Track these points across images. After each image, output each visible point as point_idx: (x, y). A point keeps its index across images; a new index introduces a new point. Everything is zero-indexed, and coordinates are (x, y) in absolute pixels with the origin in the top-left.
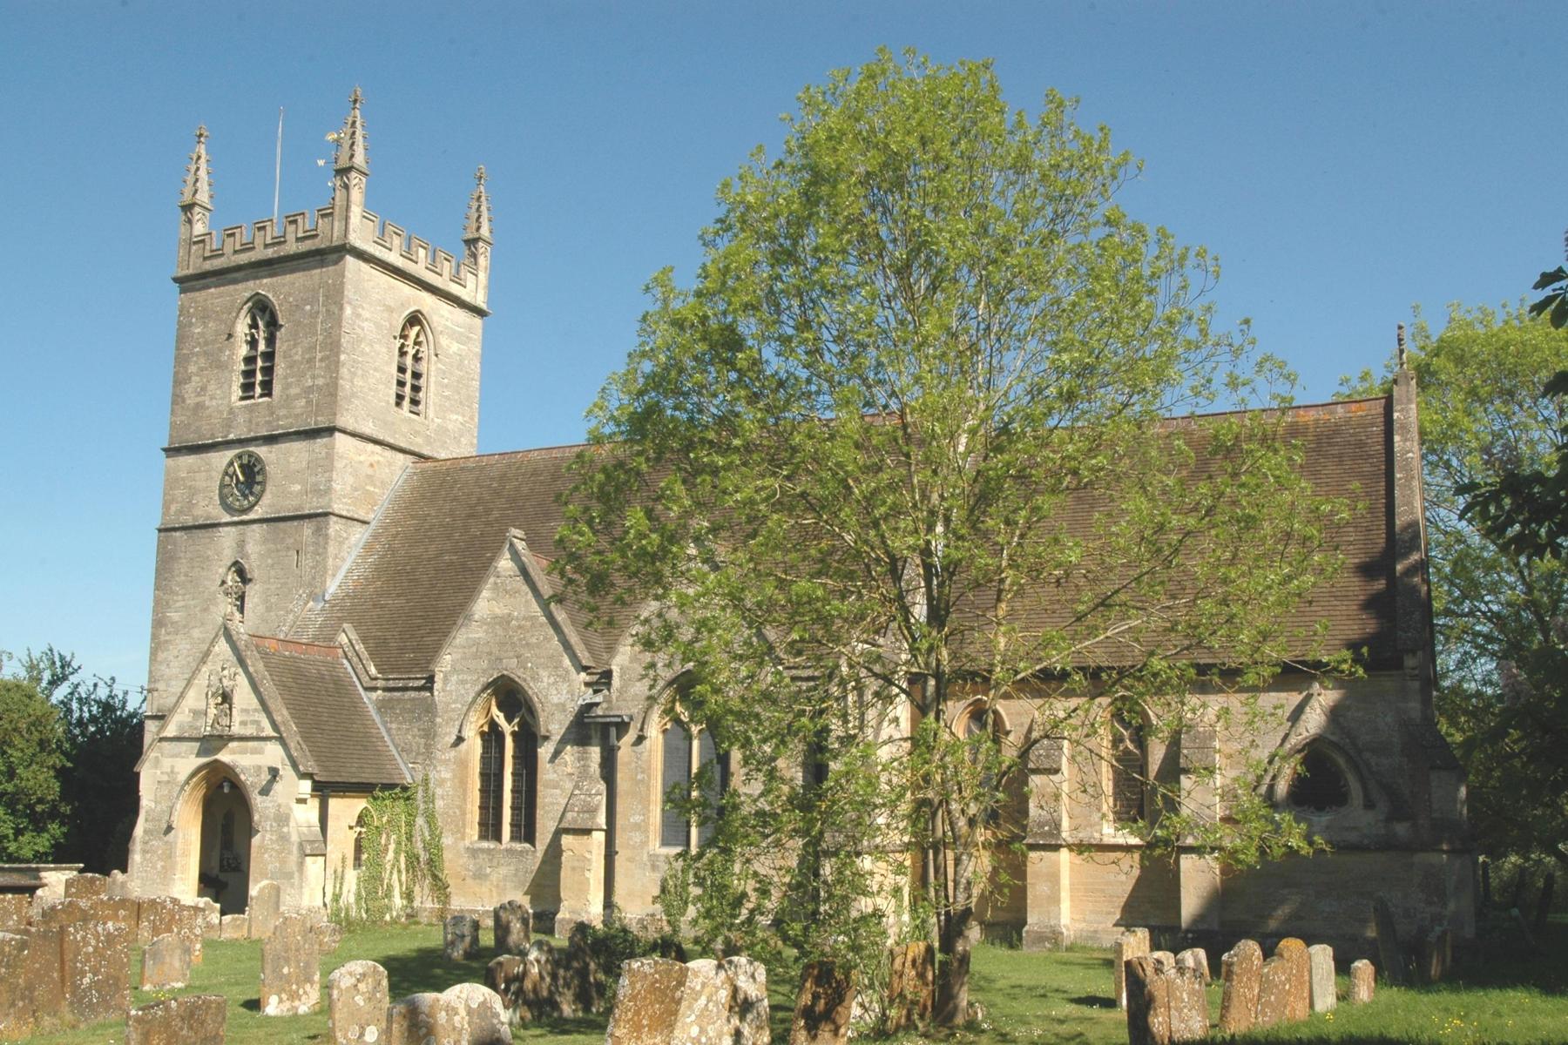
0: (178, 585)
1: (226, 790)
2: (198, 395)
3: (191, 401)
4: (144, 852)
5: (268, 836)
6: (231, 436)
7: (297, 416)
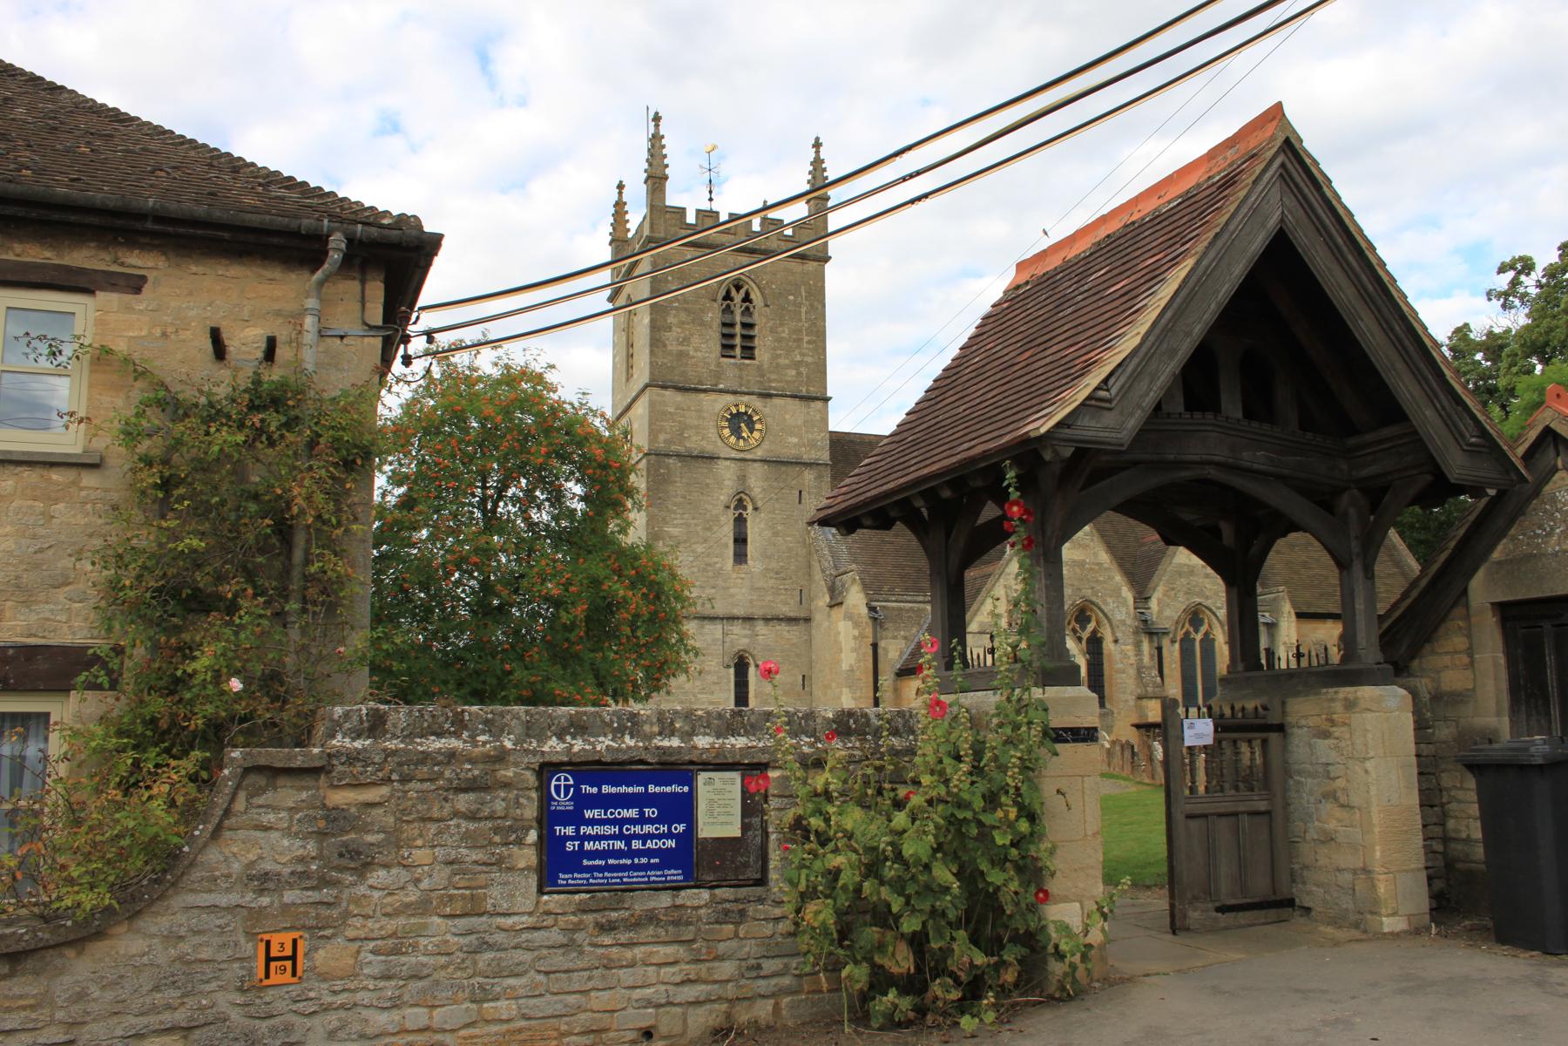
0: (675, 504)
2: (681, 344)
3: (673, 347)
6: (721, 386)
7: (788, 382)
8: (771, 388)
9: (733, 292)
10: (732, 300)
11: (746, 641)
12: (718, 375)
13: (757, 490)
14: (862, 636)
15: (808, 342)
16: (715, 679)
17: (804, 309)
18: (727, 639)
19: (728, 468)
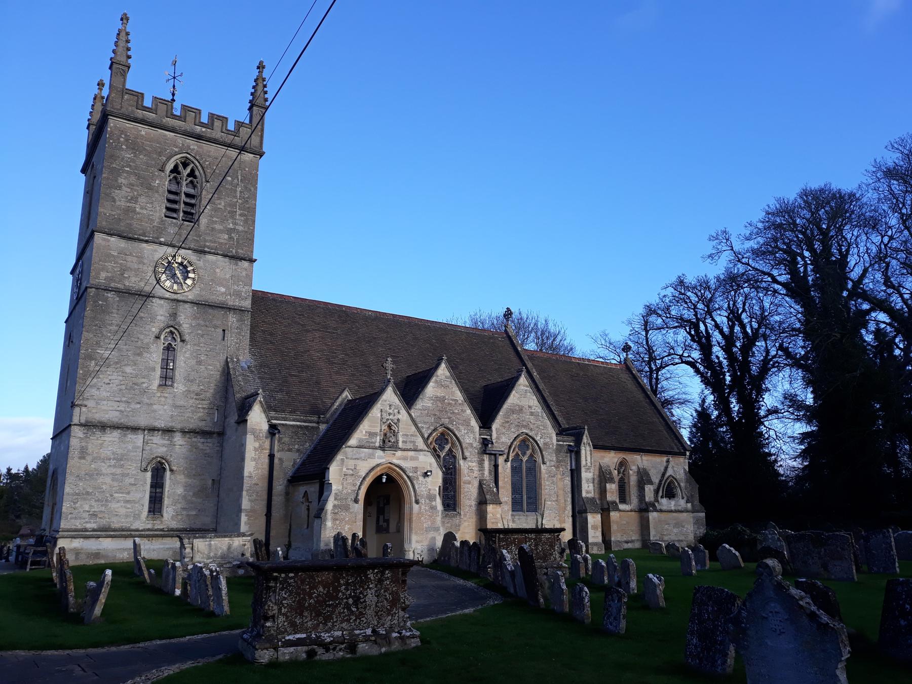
1: (384, 480)
2: (129, 201)
4: (334, 520)
5: (423, 507)
6: (162, 240)
8: (205, 246)
9: (181, 168)
10: (179, 173)
11: (164, 449)
12: (160, 230)
13: (184, 325)
14: (261, 448)
15: (240, 215)
16: (132, 481)
17: (239, 189)
18: (147, 448)
19: (162, 306)
